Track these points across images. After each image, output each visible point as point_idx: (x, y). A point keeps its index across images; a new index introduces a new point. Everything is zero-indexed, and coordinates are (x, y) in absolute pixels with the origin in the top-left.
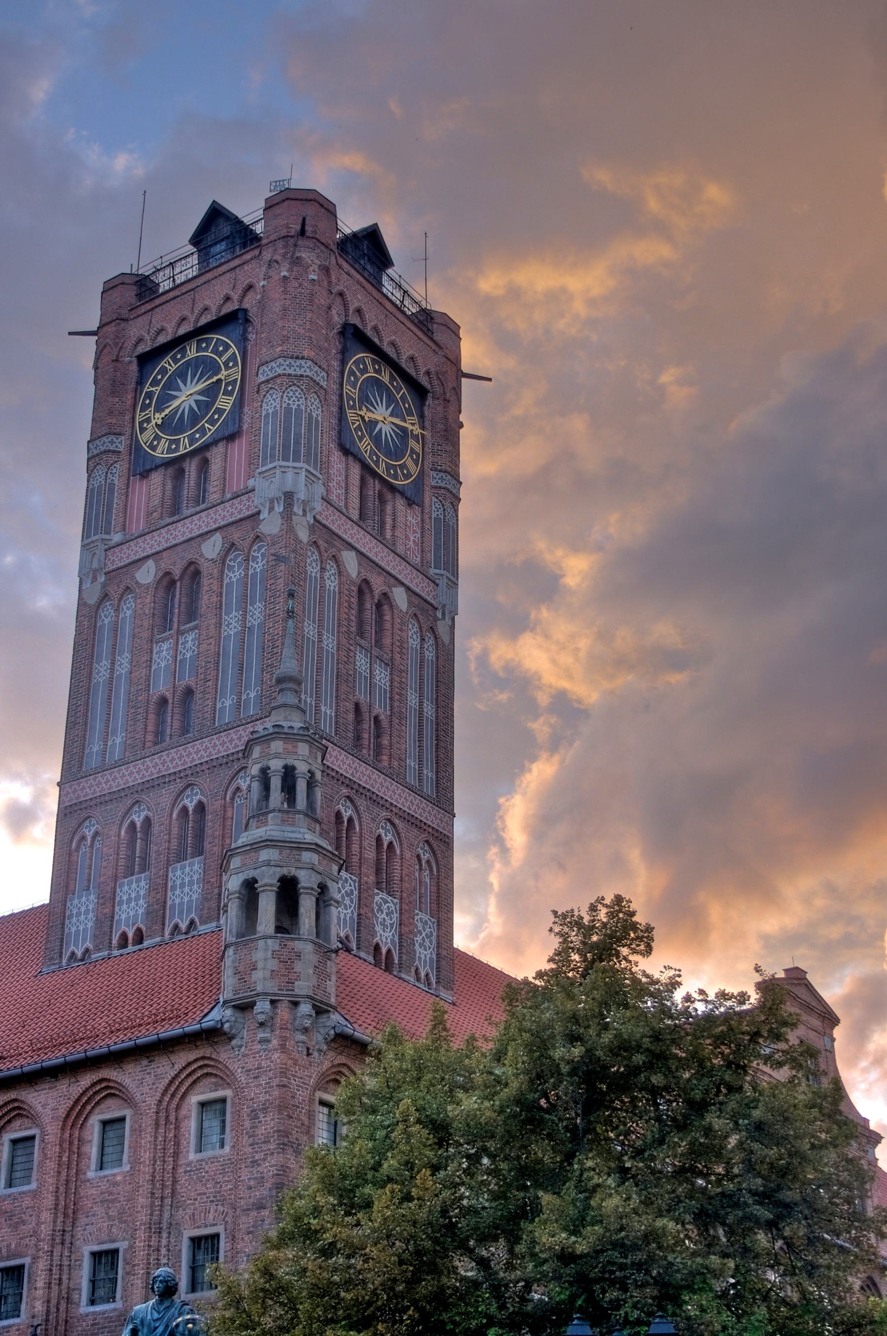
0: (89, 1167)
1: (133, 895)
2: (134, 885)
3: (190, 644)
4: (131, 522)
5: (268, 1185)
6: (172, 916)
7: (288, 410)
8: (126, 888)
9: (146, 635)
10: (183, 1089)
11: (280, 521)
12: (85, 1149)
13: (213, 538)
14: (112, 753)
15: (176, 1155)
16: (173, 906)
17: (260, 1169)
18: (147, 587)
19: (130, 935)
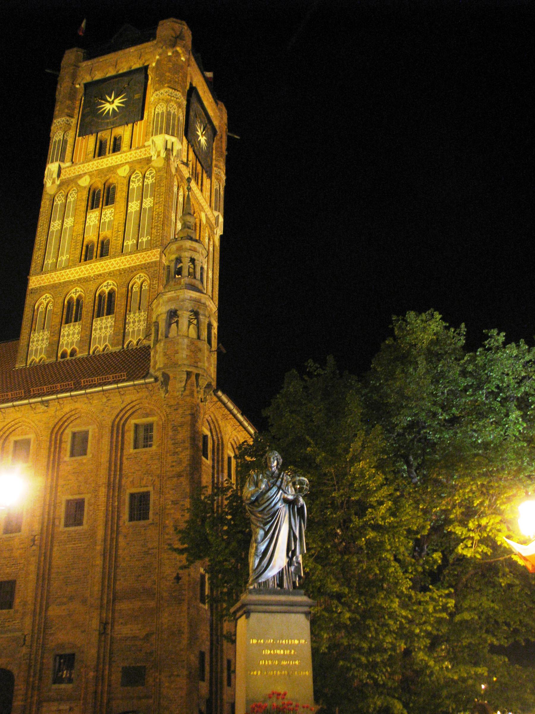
0: (65, 455)
1: (71, 332)
2: (72, 327)
3: (108, 215)
4: (76, 158)
5: (184, 465)
6: (94, 344)
7: (169, 113)
8: (67, 329)
9: (84, 209)
10: (127, 416)
11: (163, 161)
12: (63, 445)
13: (124, 168)
14: (61, 265)
15: (122, 449)
16: (95, 338)
17: (180, 456)
18: (85, 187)
19: (69, 351)
